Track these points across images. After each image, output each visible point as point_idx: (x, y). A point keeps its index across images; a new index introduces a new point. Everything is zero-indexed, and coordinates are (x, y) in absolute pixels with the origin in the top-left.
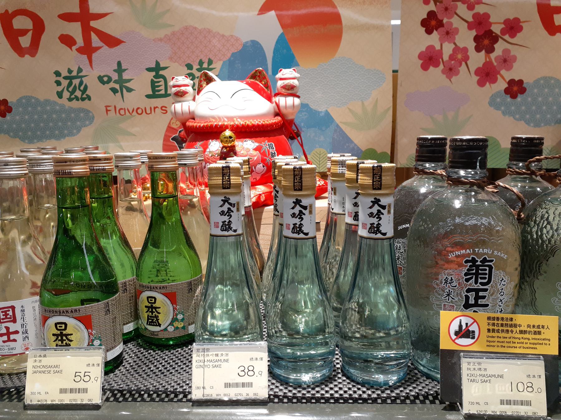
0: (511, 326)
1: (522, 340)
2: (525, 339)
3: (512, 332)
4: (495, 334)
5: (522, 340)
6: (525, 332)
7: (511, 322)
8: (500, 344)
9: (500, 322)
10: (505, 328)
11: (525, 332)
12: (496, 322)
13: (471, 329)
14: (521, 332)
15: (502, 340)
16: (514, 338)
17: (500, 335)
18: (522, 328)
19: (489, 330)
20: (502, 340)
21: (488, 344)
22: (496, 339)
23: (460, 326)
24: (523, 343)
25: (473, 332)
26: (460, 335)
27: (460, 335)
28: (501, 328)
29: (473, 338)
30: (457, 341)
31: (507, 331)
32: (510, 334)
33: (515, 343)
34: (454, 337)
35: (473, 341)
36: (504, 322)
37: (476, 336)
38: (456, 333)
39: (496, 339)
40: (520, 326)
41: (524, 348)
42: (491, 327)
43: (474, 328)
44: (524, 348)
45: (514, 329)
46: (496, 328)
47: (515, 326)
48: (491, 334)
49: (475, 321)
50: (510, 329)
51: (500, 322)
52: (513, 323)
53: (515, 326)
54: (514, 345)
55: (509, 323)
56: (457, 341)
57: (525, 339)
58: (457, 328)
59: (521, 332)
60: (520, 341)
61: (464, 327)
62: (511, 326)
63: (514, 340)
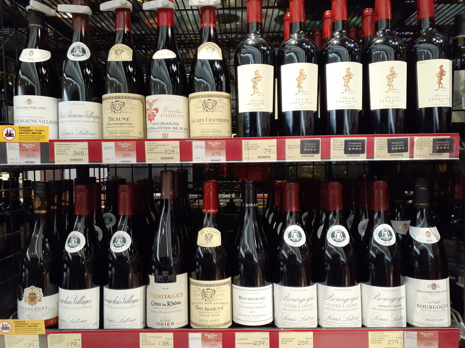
1: (33, 137)
2: (35, 136)
3: (29, 133)
5: (33, 137)
6: (34, 133)
11: (34, 133)
14: (33, 133)
16: (30, 136)
18: (33, 132)
24: (34, 138)
33: (30, 138)
40: (32, 130)
41: (34, 140)
44: (34, 140)
45: (30, 132)
47: (30, 131)
52: (29, 129)
53: (30, 131)
57: (35, 136)
59: (33, 133)
60: (32, 137)
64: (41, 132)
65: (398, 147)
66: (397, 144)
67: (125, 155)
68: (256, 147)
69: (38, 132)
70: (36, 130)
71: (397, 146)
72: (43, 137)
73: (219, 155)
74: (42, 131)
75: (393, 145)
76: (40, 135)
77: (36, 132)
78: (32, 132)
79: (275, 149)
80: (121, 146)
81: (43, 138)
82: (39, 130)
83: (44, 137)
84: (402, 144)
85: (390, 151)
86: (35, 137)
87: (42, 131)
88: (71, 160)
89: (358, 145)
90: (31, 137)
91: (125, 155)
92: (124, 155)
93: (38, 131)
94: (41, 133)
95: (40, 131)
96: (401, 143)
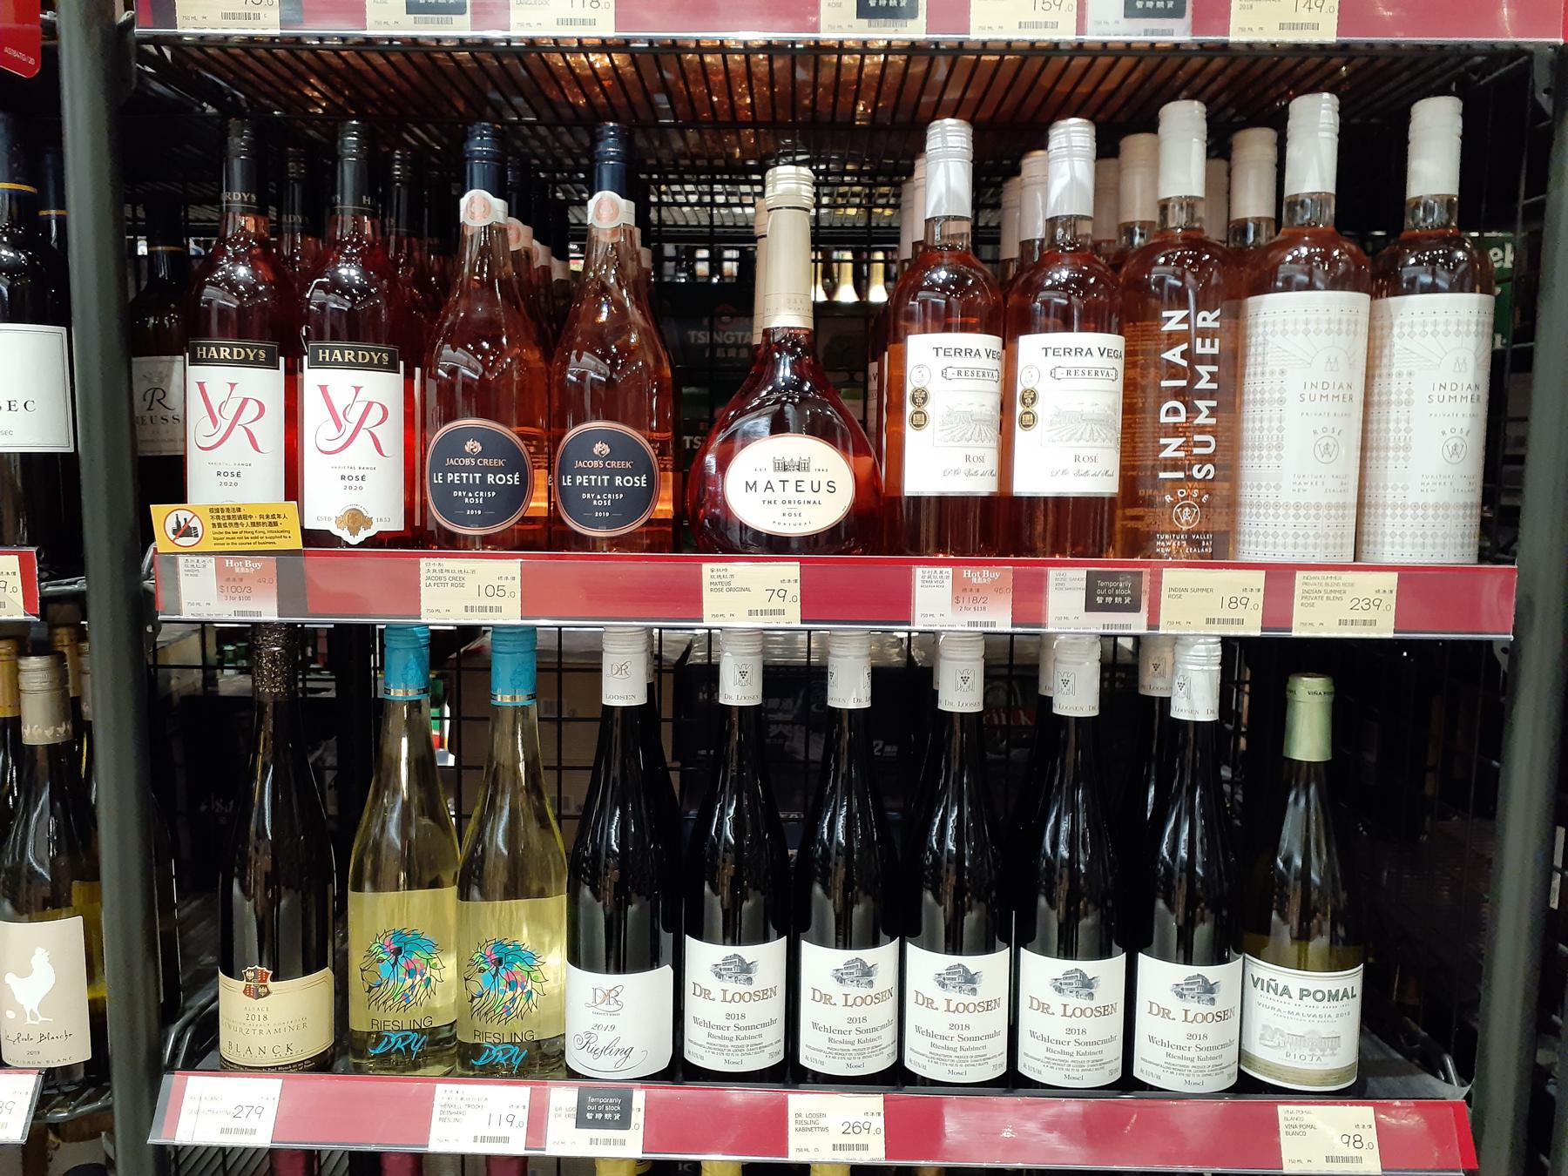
0: (240, 517)
1: (256, 535)
4: (223, 529)
7: (237, 514)
8: (230, 541)
9: (226, 514)
10: (233, 522)
12: (220, 514)
13: (191, 525)
14: (253, 524)
15: (232, 535)
17: (228, 530)
19: (214, 524)
20: (232, 535)
21: (216, 541)
22: (224, 535)
23: (178, 523)
25: (195, 528)
26: (180, 533)
27: (180, 533)
28: (228, 522)
29: (197, 536)
30: (176, 541)
31: (237, 523)
32: (240, 528)
34: (173, 537)
35: (198, 539)
36: (231, 514)
37: (200, 535)
38: (175, 532)
39: (224, 535)
40: (251, 517)
42: (216, 521)
43: (194, 523)
45: (244, 521)
46: (222, 521)
47: (245, 517)
48: (217, 530)
49: (195, 515)
50: (239, 522)
51: (226, 514)
52: (241, 513)
53: (245, 517)
54: (247, 541)
55: (237, 514)
56: (176, 541)
58: (175, 526)
59: (253, 524)
61: (183, 524)
62: (240, 517)
63: (247, 535)
64: (277, 520)
69: (266, 521)
70: (261, 516)
72: (283, 534)
74: (279, 516)
76: (274, 528)
77: (262, 520)
78: (249, 521)
81: (285, 537)
82: (270, 514)
83: (288, 535)
86: (262, 535)
87: (279, 516)
90: (250, 535)
93: (268, 517)
94: (276, 524)
95: (273, 517)
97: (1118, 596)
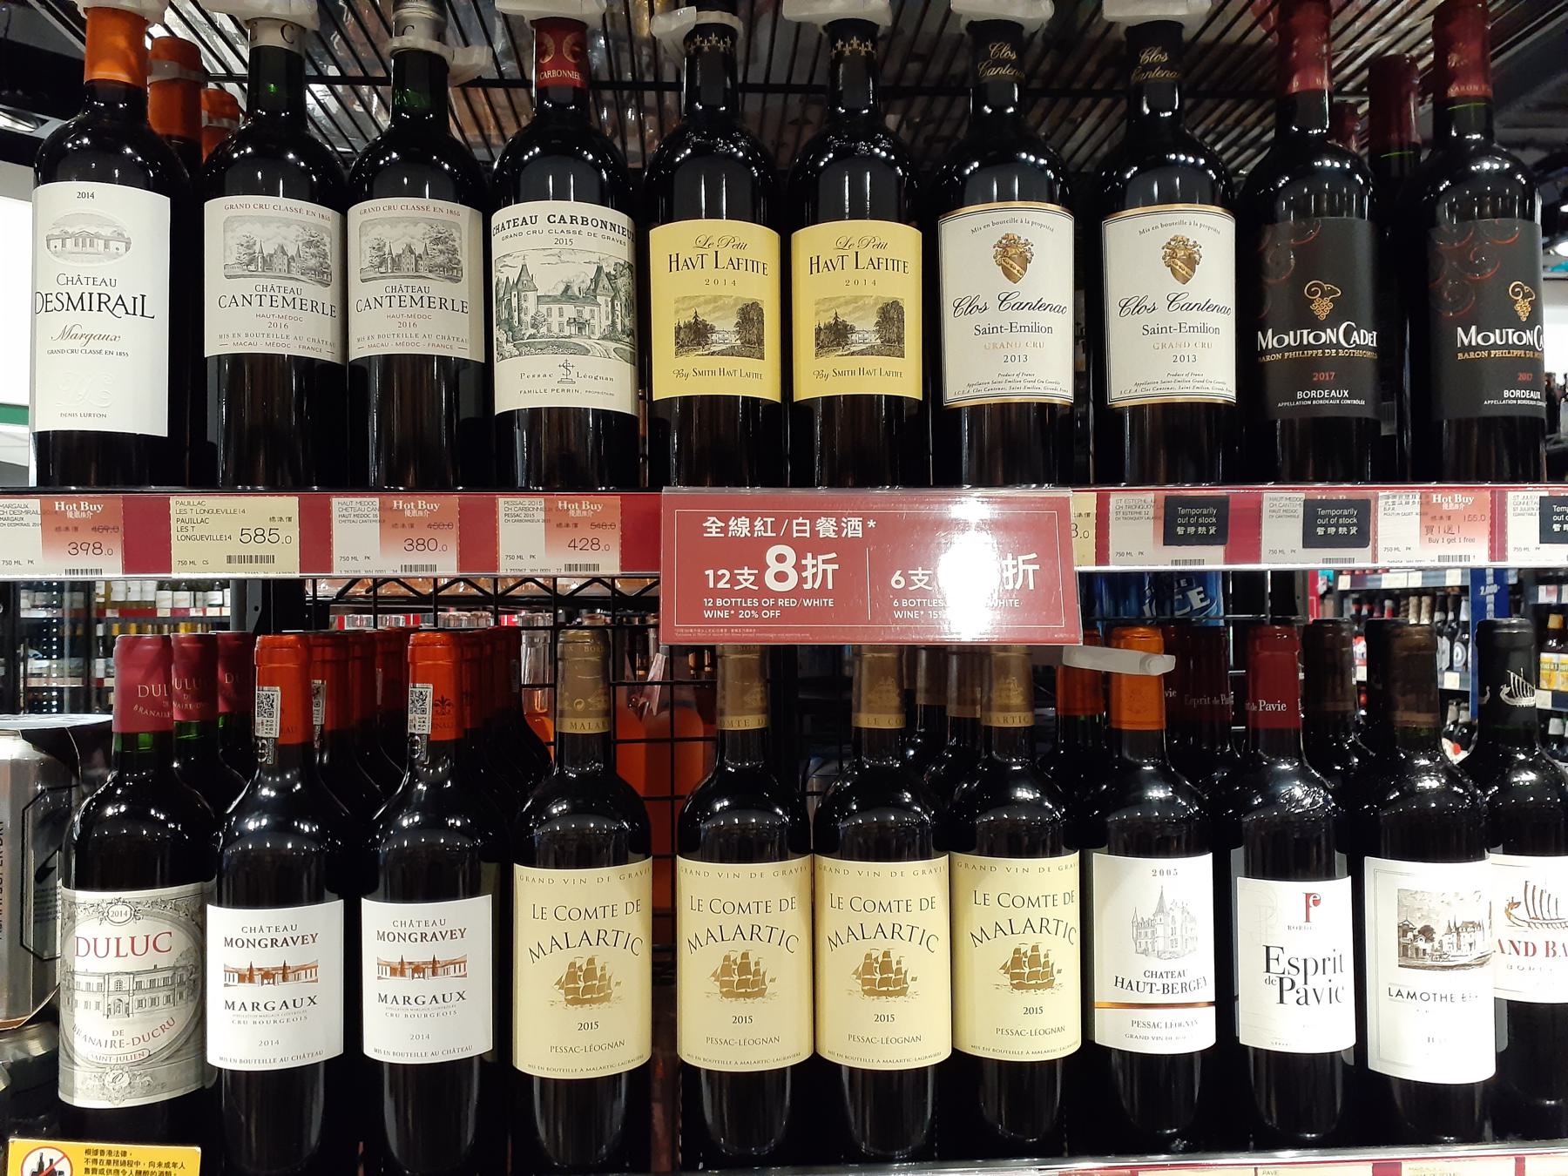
65: (1197, 525)
66: (1334, 517)
67: (415, 544)
68: (215, 526)
71: (1333, 521)
73: (595, 547)
75: (1183, 516)
79: (292, 531)
80: (403, 510)
84: (1349, 516)
85: (1170, 538)
88: (230, 560)
89: (1205, 516)
91: (415, 544)
92: (410, 542)
96: (1346, 512)
97: (1343, 525)
